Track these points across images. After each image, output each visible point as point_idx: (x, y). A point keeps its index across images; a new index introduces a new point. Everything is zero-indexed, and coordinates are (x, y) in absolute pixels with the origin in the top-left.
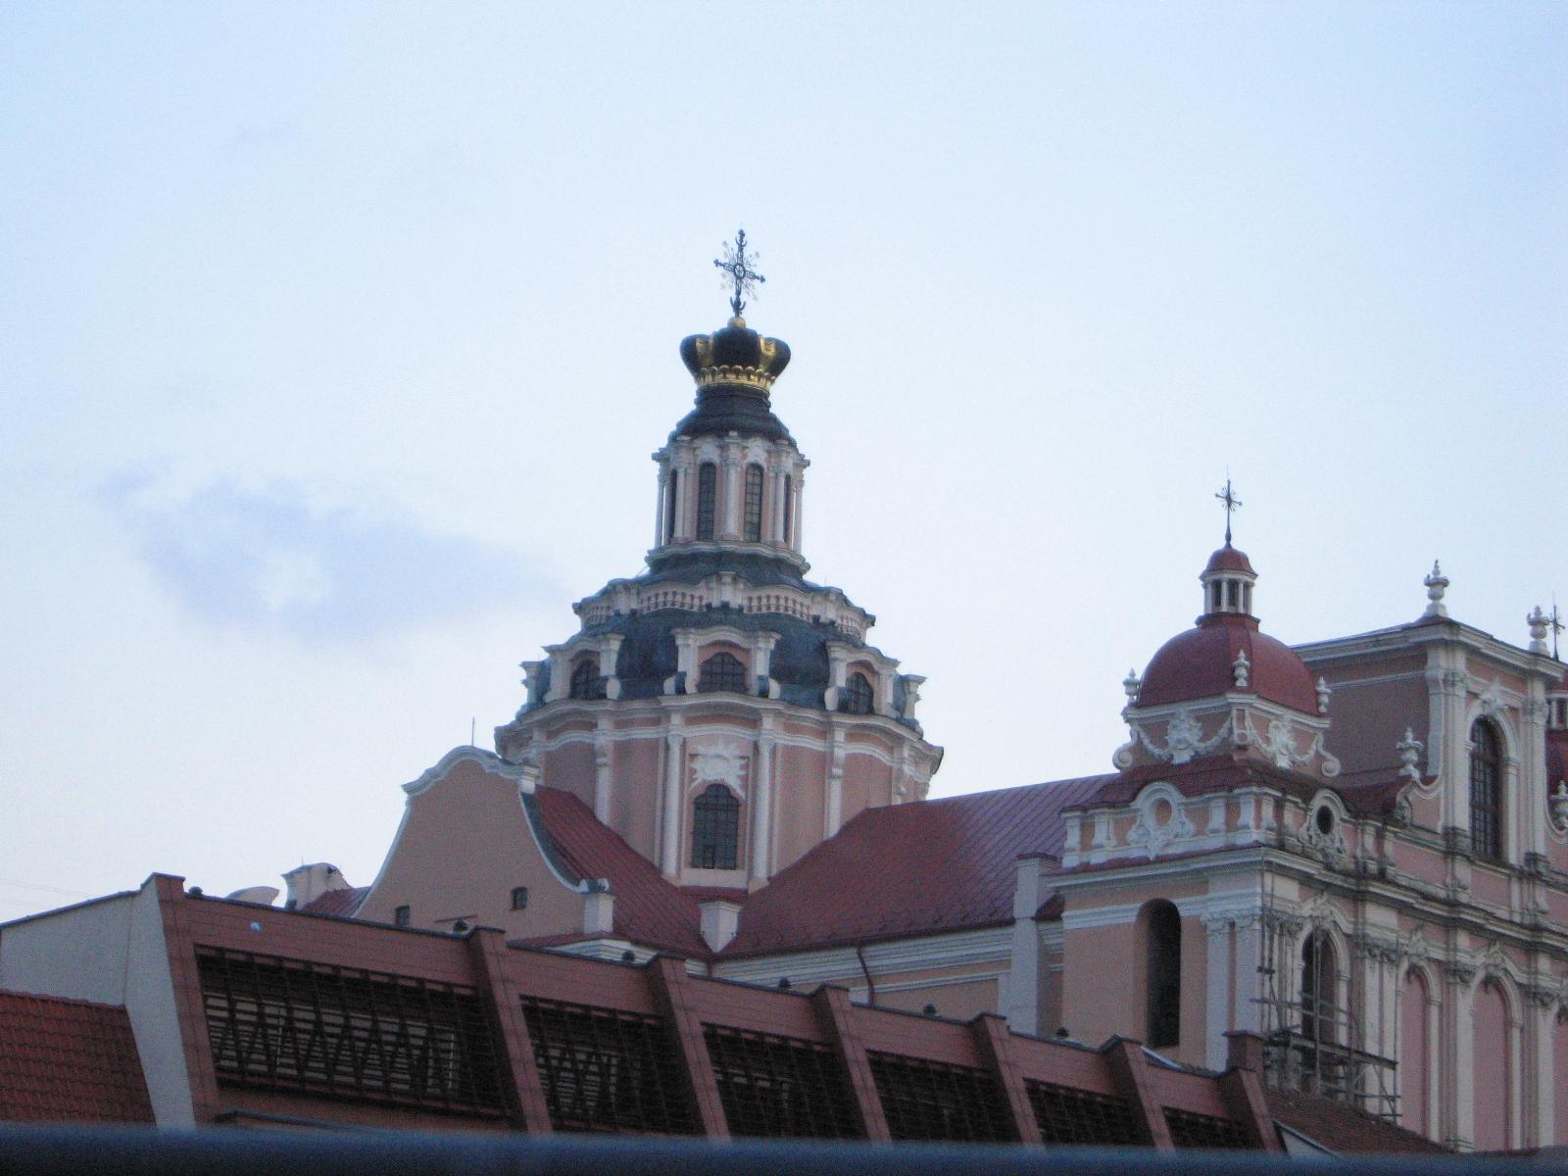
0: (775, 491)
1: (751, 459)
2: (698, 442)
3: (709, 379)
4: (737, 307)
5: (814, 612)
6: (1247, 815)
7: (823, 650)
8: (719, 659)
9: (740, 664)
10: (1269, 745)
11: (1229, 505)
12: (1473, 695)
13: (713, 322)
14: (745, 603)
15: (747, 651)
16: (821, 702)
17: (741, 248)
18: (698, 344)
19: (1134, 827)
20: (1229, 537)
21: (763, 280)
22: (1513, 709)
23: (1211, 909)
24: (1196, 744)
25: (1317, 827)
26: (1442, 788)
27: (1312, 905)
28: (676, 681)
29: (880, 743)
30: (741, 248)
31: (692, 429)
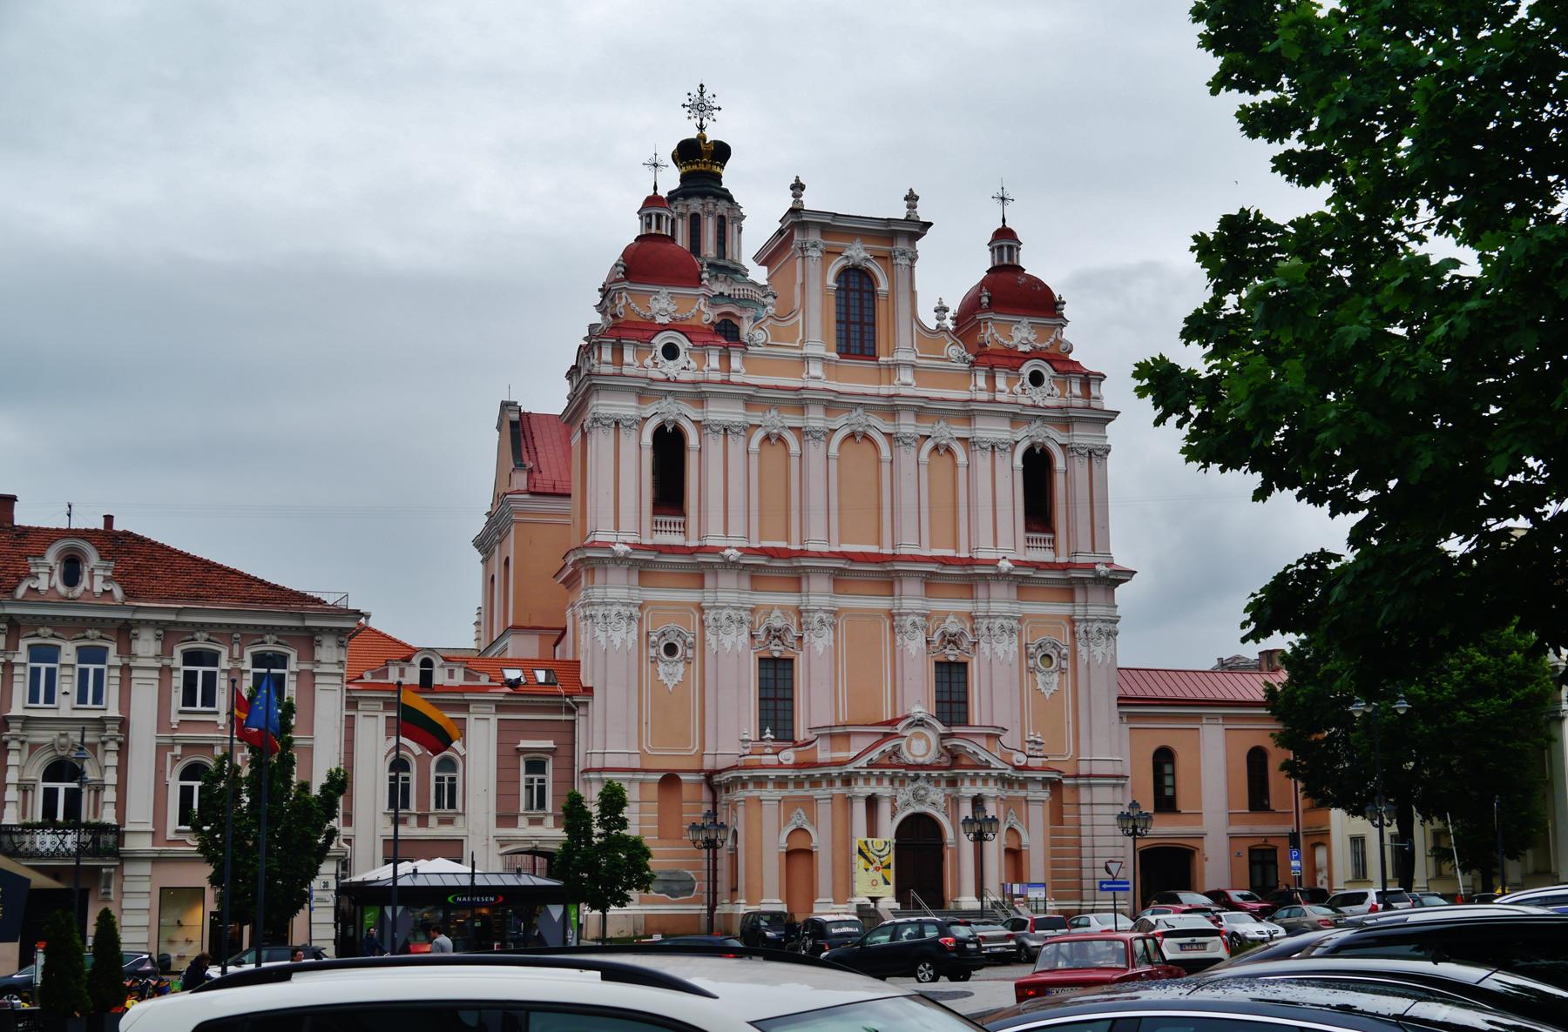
1: (692, 211)
4: (701, 128)
12: (830, 253)
17: (702, 94)
21: (719, 109)
26: (800, 317)
30: (702, 94)
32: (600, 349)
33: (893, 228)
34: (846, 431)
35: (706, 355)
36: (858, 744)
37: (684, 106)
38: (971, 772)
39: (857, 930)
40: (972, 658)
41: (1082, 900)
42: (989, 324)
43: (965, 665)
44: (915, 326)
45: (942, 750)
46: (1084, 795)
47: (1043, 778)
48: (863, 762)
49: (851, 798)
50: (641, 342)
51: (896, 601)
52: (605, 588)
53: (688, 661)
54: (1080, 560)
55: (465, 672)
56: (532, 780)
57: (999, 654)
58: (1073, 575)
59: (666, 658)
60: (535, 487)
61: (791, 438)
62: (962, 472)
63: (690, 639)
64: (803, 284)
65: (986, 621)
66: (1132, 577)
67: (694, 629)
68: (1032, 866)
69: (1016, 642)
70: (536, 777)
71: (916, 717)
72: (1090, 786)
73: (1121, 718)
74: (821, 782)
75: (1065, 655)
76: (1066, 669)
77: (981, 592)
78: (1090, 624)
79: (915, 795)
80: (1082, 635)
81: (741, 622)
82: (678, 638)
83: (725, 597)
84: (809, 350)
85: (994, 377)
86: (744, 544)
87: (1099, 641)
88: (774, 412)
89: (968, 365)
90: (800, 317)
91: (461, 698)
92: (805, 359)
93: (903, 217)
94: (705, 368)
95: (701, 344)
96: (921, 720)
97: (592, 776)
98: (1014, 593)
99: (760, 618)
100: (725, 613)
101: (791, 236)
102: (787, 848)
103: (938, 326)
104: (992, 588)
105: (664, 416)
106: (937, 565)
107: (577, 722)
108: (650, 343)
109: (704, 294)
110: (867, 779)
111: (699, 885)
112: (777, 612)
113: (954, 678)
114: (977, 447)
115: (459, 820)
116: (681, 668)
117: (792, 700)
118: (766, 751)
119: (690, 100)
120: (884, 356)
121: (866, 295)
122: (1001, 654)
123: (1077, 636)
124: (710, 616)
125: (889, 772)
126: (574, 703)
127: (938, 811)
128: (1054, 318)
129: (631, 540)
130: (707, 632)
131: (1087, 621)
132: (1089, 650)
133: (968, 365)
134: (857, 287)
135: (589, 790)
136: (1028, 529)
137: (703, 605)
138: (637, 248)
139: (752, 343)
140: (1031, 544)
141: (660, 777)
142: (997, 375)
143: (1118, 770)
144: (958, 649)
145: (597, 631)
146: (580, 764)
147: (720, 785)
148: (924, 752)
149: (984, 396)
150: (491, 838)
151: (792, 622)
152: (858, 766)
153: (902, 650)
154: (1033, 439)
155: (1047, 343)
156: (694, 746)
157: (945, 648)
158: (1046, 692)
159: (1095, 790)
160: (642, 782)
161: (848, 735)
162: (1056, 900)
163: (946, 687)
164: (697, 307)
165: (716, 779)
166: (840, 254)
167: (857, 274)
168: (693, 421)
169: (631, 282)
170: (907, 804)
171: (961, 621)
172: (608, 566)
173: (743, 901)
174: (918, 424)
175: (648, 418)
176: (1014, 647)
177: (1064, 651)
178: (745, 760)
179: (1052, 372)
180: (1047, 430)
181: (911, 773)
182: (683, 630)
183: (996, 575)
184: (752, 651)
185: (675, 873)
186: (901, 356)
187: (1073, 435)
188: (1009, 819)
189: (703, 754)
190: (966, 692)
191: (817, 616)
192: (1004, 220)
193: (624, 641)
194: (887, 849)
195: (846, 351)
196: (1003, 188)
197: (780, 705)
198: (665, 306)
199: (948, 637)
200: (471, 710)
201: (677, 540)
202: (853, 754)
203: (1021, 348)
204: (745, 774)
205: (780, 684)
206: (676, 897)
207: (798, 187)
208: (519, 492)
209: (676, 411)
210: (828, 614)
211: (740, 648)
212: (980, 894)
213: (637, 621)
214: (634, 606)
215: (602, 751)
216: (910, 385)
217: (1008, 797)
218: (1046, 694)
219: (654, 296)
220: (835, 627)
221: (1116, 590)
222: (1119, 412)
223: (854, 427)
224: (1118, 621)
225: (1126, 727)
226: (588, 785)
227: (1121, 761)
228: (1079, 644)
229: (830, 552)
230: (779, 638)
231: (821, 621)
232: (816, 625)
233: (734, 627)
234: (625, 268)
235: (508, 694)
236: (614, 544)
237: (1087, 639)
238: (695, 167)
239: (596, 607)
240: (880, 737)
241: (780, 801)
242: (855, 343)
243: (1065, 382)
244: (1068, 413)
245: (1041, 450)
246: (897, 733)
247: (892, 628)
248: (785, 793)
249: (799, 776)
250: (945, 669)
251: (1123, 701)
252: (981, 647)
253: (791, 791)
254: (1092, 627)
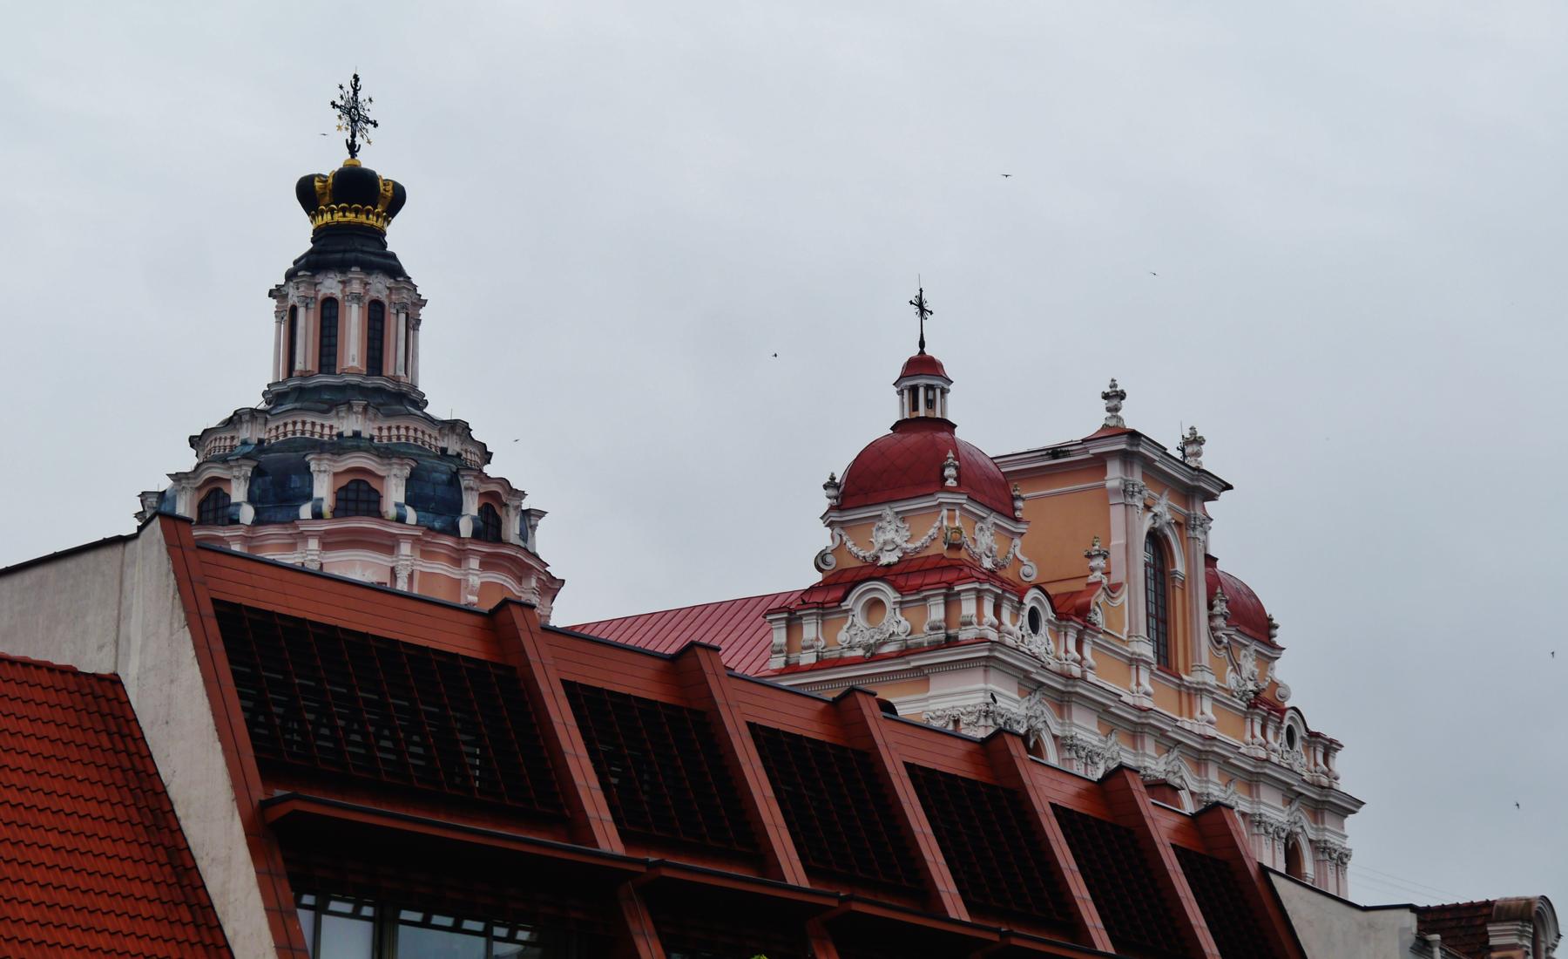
0: (396, 325)
1: (373, 295)
2: (319, 278)
3: (327, 218)
4: (352, 148)
5: (441, 444)
6: (968, 608)
7: (454, 481)
8: (354, 486)
9: (377, 491)
10: (976, 547)
11: (922, 315)
13: (329, 161)
14: (376, 433)
15: (382, 478)
16: (454, 530)
18: (317, 184)
19: (845, 627)
20: (922, 344)
21: (376, 125)
22: (1178, 524)
23: (933, 707)
24: (904, 545)
25: (1028, 628)
27: (1027, 704)
28: (312, 506)
29: (509, 572)
31: (310, 266)
90: (1125, 597)
238: (362, 218)
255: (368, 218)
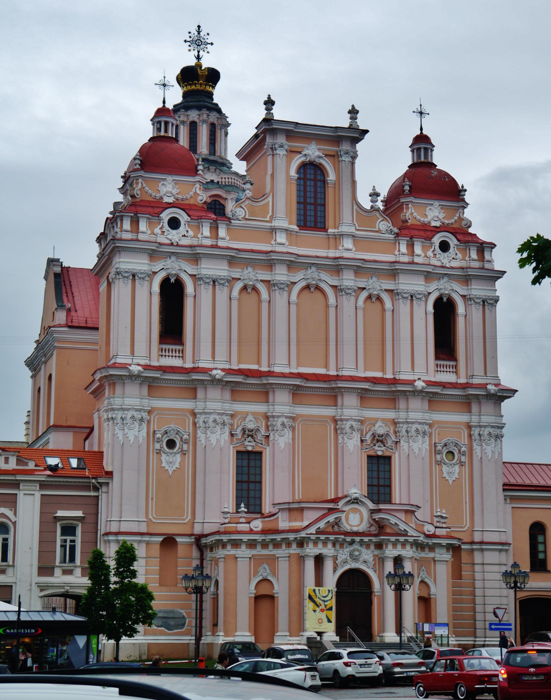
1: (191, 119)
4: (198, 58)
12: (292, 152)
17: (199, 33)
26: (270, 199)
30: (199, 33)
32: (122, 220)
33: (339, 134)
34: (303, 284)
35: (201, 226)
36: (310, 516)
37: (185, 41)
38: (393, 539)
39: (307, 657)
40: (395, 453)
41: (476, 637)
42: (410, 206)
43: (389, 458)
44: (355, 207)
45: (372, 522)
46: (478, 557)
47: (447, 544)
48: (313, 530)
49: (303, 557)
50: (152, 216)
51: (339, 410)
52: (123, 398)
53: (183, 453)
54: (475, 381)
55: (17, 459)
56: (65, 541)
57: (415, 450)
58: (470, 392)
59: (167, 450)
60: (72, 322)
61: (261, 287)
62: (388, 315)
63: (185, 437)
64: (272, 175)
65: (405, 426)
66: (514, 394)
67: (189, 429)
68: (438, 611)
69: (428, 441)
70: (69, 538)
71: (352, 497)
72: (482, 550)
73: (505, 499)
74: (281, 544)
75: (464, 452)
76: (465, 462)
77: (402, 404)
78: (483, 429)
79: (351, 555)
80: (477, 437)
81: (224, 424)
82: (177, 436)
83: (211, 406)
84: (276, 223)
85: (413, 245)
86: (227, 367)
87: (489, 442)
88: (250, 269)
89: (394, 236)
90: (270, 199)
91: (13, 478)
92: (273, 230)
93: (347, 125)
94: (199, 236)
95: (196, 218)
96: (356, 499)
97: (111, 538)
98: (426, 405)
99: (237, 422)
100: (212, 417)
101: (264, 139)
102: (255, 594)
103: (372, 207)
104: (410, 401)
105: (169, 271)
106: (369, 384)
107: (100, 497)
108: (159, 217)
109: (199, 181)
110: (315, 543)
111: (189, 621)
112: (250, 417)
113: (381, 468)
114: (400, 297)
115: (10, 571)
116: (178, 458)
117: (260, 482)
118: (241, 520)
119: (190, 37)
120: (332, 229)
121: (319, 184)
122: (416, 451)
123: (473, 438)
124: (200, 419)
125: (332, 537)
126: (98, 483)
127: (368, 567)
128: (458, 201)
129: (143, 362)
130: (198, 432)
131: (480, 426)
132: (482, 448)
133: (394, 236)
134: (312, 177)
135: (108, 549)
136: (437, 358)
137: (196, 411)
138: (150, 147)
139: (234, 217)
140: (439, 369)
141: (161, 539)
142: (415, 243)
143: (503, 539)
144: (384, 446)
145: (117, 430)
146: (102, 528)
147: (206, 546)
148: (359, 523)
149: (406, 259)
150: (33, 584)
151: (262, 425)
152: (309, 532)
153: (343, 446)
154: (442, 291)
155: (453, 220)
156: (187, 516)
157: (375, 445)
158: (449, 479)
159: (486, 553)
160: (148, 543)
161: (302, 509)
162: (456, 636)
163: (375, 474)
164: (194, 190)
165: (204, 541)
166: (300, 153)
167: (312, 167)
168: (190, 275)
169: (145, 171)
170: (345, 562)
171: (386, 425)
172: (126, 381)
173: (222, 634)
174: (357, 279)
175: (157, 272)
176: (426, 446)
177: (463, 449)
178: (225, 527)
179: (456, 242)
180: (451, 284)
181: (349, 539)
182: (181, 430)
183: (413, 392)
184: (231, 446)
185: (172, 612)
186: (344, 229)
187: (471, 289)
188: (421, 574)
189: (194, 523)
190: (390, 478)
191: (280, 420)
192: (421, 129)
193: (136, 437)
194: (330, 595)
195: (303, 225)
196: (421, 105)
197: (252, 486)
198: (170, 189)
199: (377, 437)
200: (21, 487)
201: (176, 362)
202: (306, 523)
203: (433, 224)
204: (225, 538)
205: (252, 471)
206: (172, 630)
207: (269, 103)
208: (60, 326)
209: (178, 268)
210: (288, 419)
211: (222, 443)
212: (399, 630)
213: (146, 423)
214: (144, 412)
215: (119, 519)
216: (351, 250)
217: (420, 557)
218: (449, 481)
219: (162, 182)
220: (293, 429)
221: (502, 404)
222: (505, 272)
223: (309, 281)
224: (503, 427)
225: (509, 507)
226: (108, 545)
227: (505, 532)
228: (474, 444)
229: (291, 373)
230: (252, 436)
231: (283, 424)
232: (279, 427)
233: (218, 428)
234: (141, 161)
235: (49, 476)
236: (130, 365)
237: (481, 440)
238: (193, 87)
239: (116, 412)
240: (325, 512)
241: (250, 558)
242: (310, 219)
243: (466, 249)
244: (467, 272)
245: (447, 299)
246: (338, 509)
247: (336, 430)
248: (254, 552)
249: (265, 540)
250: (375, 461)
251: (507, 487)
252: (402, 445)
253: (259, 551)
254: (484, 431)
255: (196, 87)
